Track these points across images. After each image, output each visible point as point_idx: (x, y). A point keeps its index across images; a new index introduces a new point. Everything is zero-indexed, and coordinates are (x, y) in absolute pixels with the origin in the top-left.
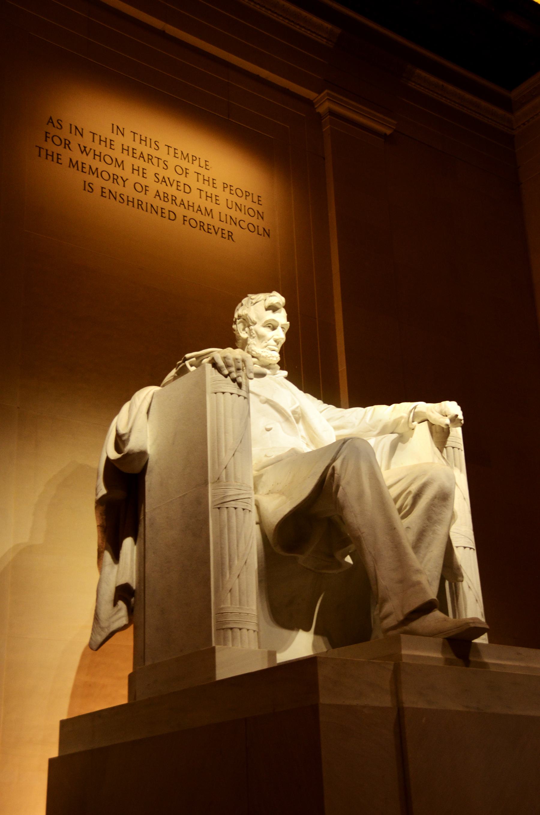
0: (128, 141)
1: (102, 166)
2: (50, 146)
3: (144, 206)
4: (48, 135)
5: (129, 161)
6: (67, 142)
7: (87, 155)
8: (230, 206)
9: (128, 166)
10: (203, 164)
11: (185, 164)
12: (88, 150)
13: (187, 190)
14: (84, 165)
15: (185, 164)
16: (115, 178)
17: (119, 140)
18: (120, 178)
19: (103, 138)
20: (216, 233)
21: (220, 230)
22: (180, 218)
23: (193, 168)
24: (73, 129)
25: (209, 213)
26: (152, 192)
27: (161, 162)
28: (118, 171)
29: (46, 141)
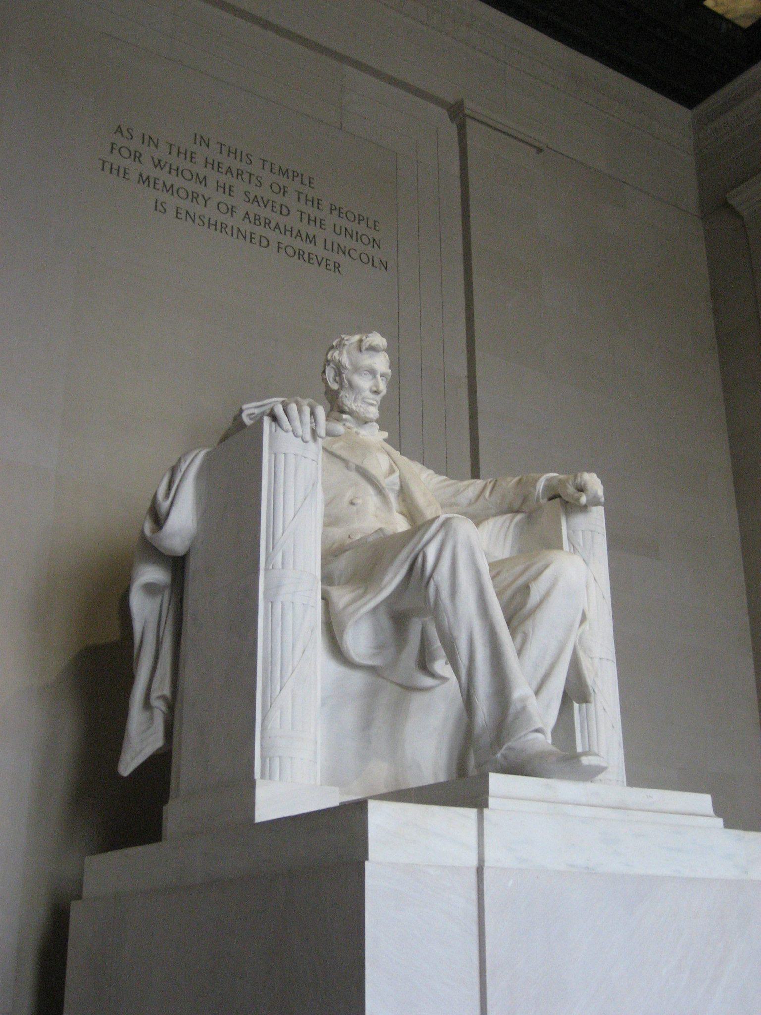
1: (178, 182)
2: (115, 159)
3: (229, 230)
4: (115, 146)
5: (213, 177)
6: (138, 155)
7: (162, 169)
8: (338, 231)
9: (212, 184)
12: (162, 163)
13: (285, 211)
14: (157, 182)
15: (283, 181)
16: (194, 197)
18: (200, 198)
20: (319, 264)
21: (324, 260)
22: (274, 245)
23: (293, 186)
24: (146, 138)
26: (239, 214)
27: (253, 179)
28: (200, 189)
29: (112, 152)
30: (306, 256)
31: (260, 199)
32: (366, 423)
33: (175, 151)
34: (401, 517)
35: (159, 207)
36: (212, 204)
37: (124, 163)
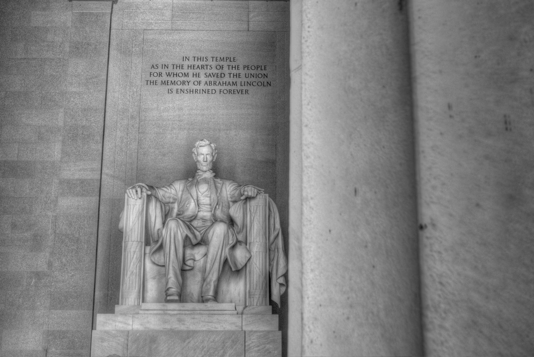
0: (191, 62)
2: (153, 79)
3: (198, 92)
5: (191, 72)
8: (247, 76)
9: (191, 75)
10: (232, 60)
11: (222, 63)
13: (223, 75)
15: (222, 63)
16: (183, 83)
17: (186, 63)
19: (178, 66)
22: (218, 92)
24: (164, 66)
25: (234, 84)
28: (185, 79)
30: (232, 92)
31: (211, 74)
32: (206, 171)
33: (175, 66)
34: (209, 206)
35: (170, 91)
36: (191, 84)
37: (155, 79)
